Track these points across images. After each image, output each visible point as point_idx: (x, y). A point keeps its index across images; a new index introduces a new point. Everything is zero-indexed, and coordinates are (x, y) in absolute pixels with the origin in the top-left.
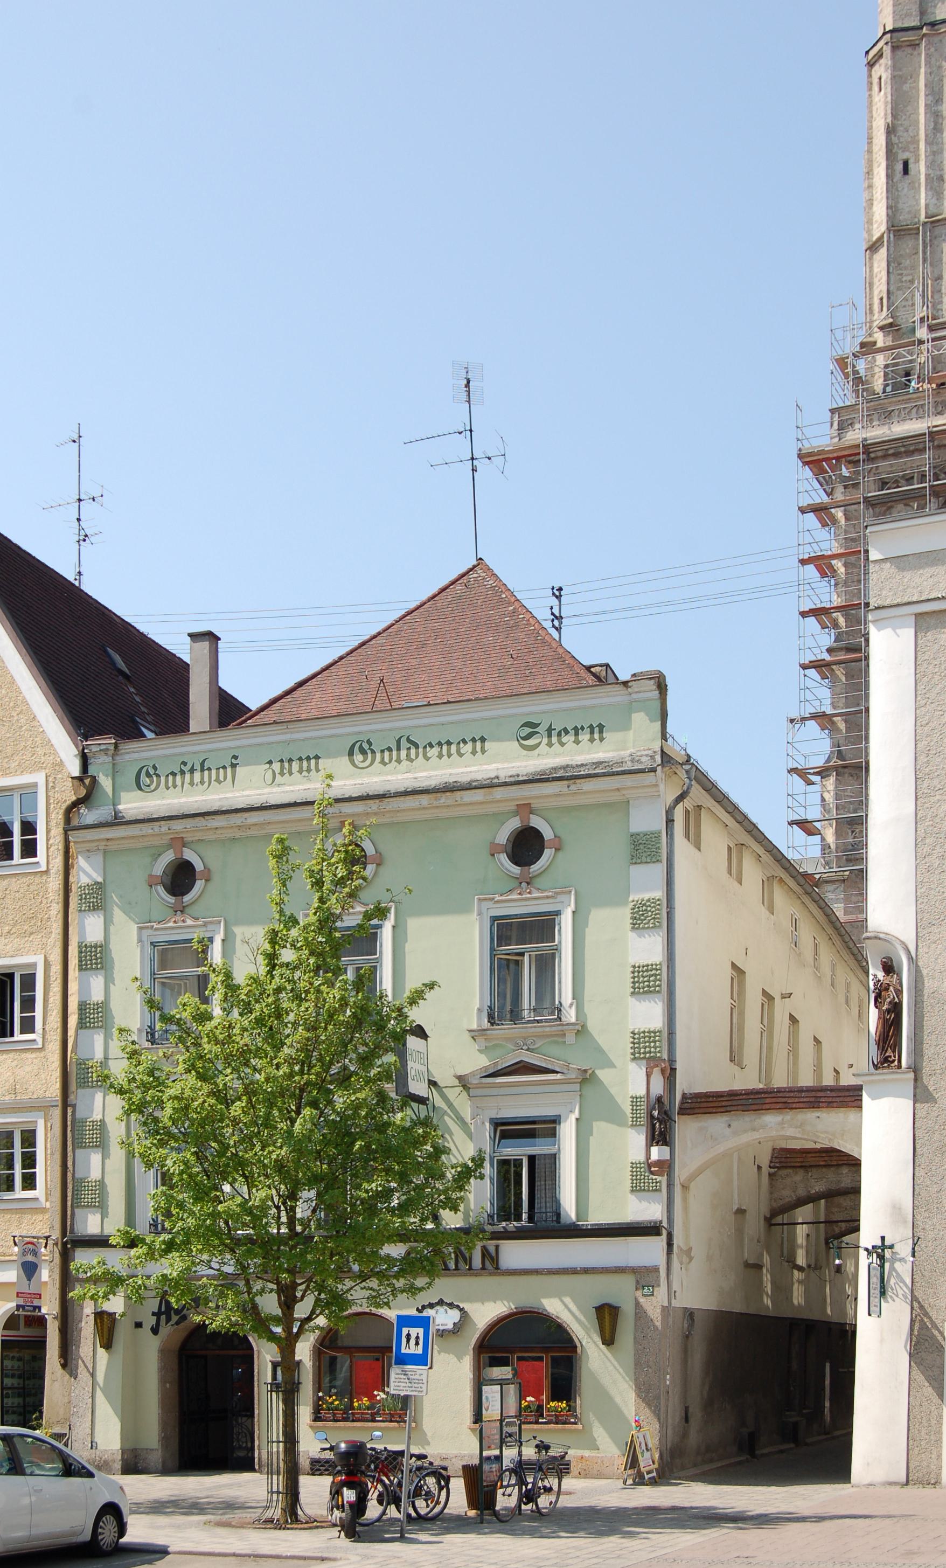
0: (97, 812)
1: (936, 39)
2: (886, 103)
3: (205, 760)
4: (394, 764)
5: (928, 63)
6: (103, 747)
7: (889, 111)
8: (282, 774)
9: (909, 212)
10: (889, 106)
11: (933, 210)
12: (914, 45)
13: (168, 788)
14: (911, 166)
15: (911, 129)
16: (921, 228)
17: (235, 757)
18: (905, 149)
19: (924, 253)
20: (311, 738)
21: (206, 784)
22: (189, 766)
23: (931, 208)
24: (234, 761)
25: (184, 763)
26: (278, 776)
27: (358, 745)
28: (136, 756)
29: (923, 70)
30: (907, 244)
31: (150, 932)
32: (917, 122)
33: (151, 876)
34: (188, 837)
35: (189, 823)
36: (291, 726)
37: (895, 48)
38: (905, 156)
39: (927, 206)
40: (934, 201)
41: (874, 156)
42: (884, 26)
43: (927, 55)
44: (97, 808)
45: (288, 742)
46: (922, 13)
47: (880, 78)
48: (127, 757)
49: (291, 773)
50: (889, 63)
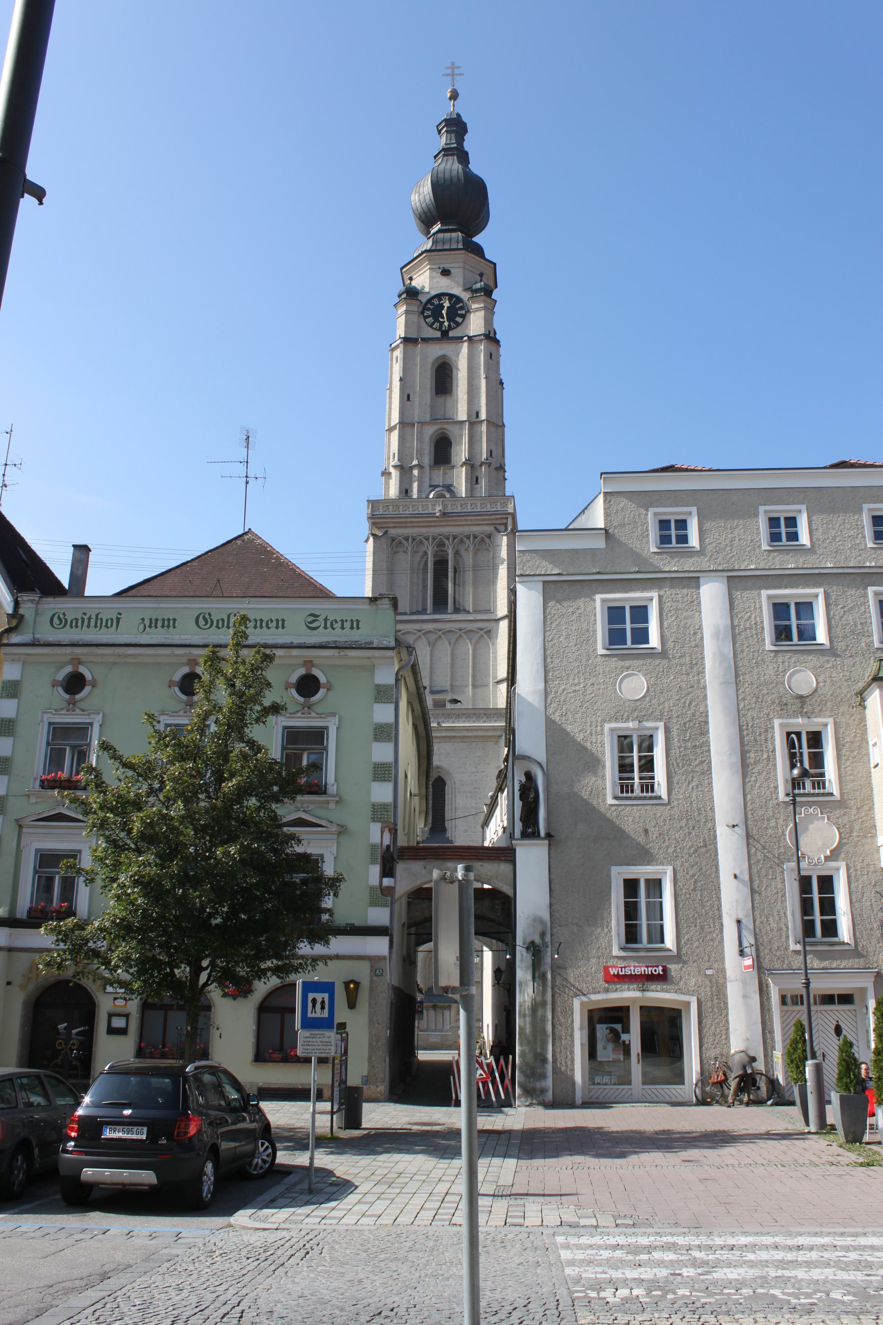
0: (23, 637)
3: (98, 614)
4: (225, 628)
6: (31, 598)
8: (150, 627)
13: (71, 627)
17: (120, 614)
20: (172, 608)
21: (98, 628)
22: (88, 616)
24: (119, 616)
25: (85, 614)
26: (147, 628)
27: (202, 615)
28: (52, 606)
31: (49, 715)
33: (54, 680)
34: (83, 659)
35: (86, 650)
36: (160, 599)
44: (22, 635)
45: (157, 608)
48: (46, 606)
49: (156, 627)
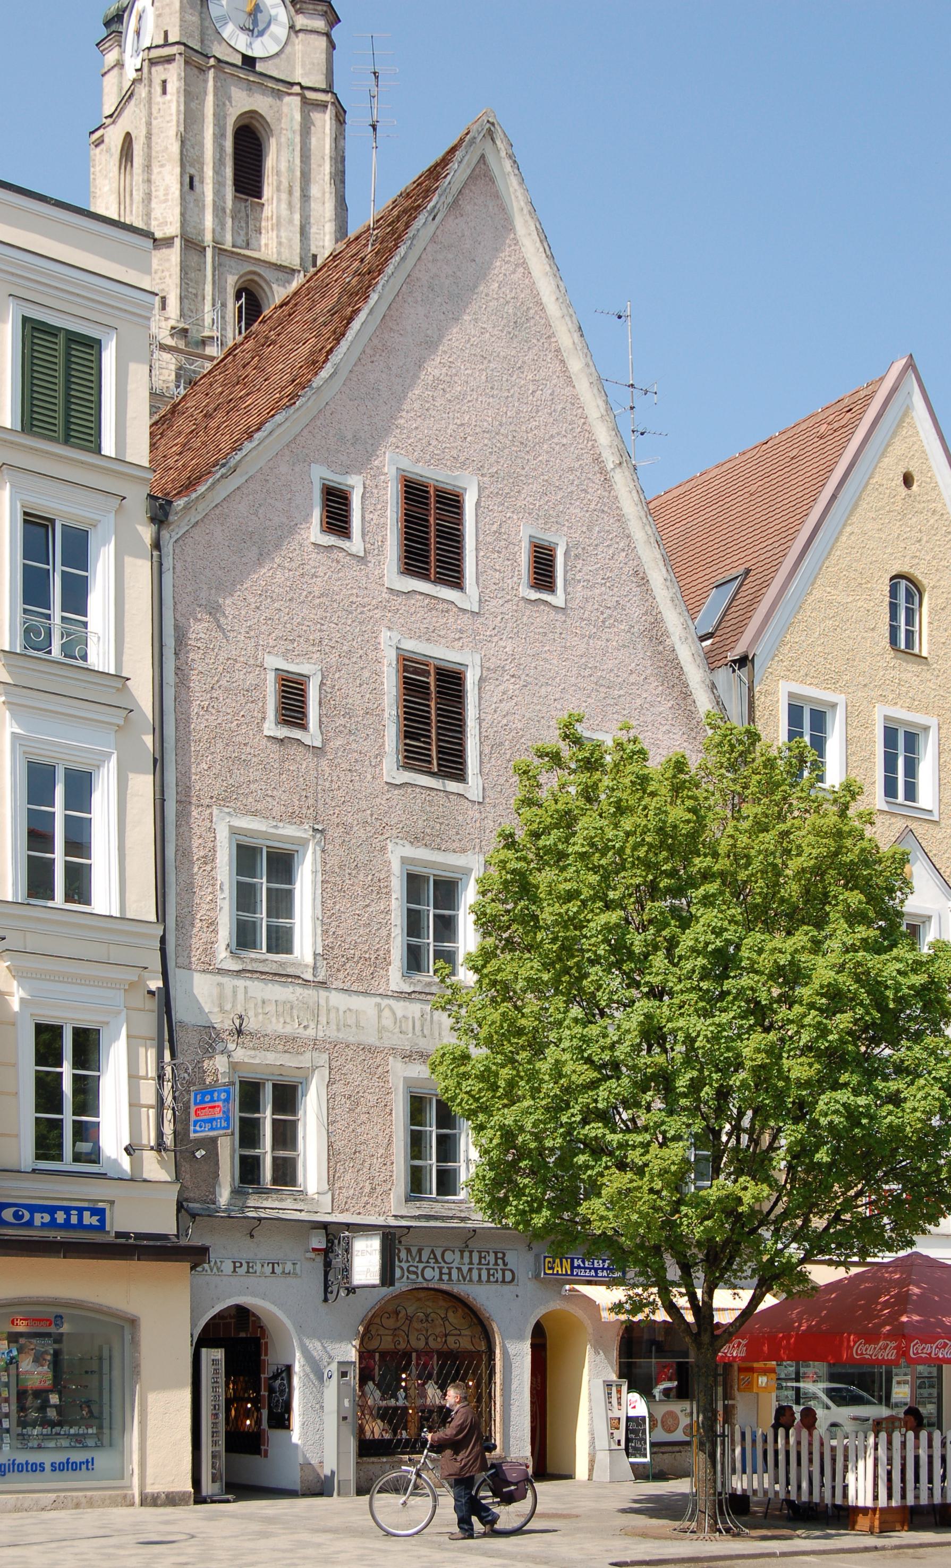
1: (222, 76)
2: (178, 111)
5: (215, 95)
7: (182, 121)
9: (195, 227)
10: (182, 117)
11: (218, 238)
12: (202, 70)
14: (196, 183)
15: (197, 148)
16: (209, 252)
18: (192, 165)
19: (214, 276)
23: (217, 234)
29: (210, 99)
30: (194, 258)
32: (202, 145)
37: (186, 62)
38: (192, 171)
39: (214, 231)
40: (218, 229)
41: (154, 154)
42: (166, 33)
43: (215, 86)
46: (202, 41)
47: (164, 82)
50: (183, 74)
